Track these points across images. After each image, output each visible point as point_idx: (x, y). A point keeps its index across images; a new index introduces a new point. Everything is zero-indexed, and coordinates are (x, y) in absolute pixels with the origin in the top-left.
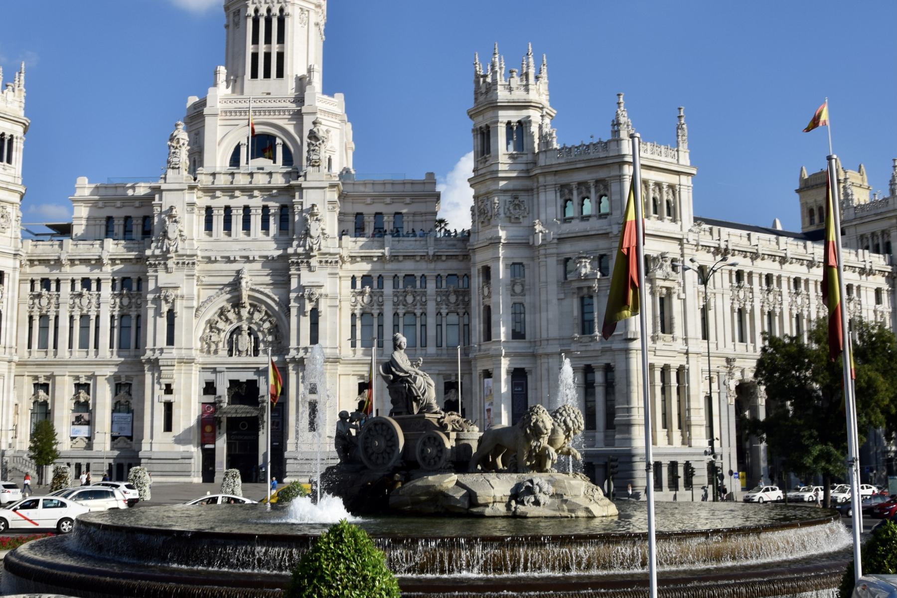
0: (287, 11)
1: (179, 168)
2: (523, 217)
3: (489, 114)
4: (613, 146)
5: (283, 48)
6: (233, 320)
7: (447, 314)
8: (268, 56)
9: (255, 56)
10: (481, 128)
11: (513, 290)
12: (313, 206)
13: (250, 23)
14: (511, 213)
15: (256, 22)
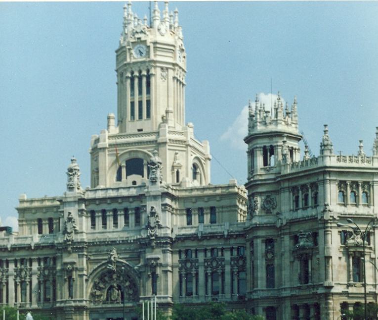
0: (150, 72)
1: (73, 188)
2: (273, 209)
3: (255, 142)
4: (320, 160)
5: (150, 97)
6: (109, 282)
7: (238, 272)
8: (140, 103)
9: (132, 104)
10: (251, 151)
11: (267, 257)
12: (152, 208)
13: (129, 81)
14: (265, 207)
15: (132, 79)
